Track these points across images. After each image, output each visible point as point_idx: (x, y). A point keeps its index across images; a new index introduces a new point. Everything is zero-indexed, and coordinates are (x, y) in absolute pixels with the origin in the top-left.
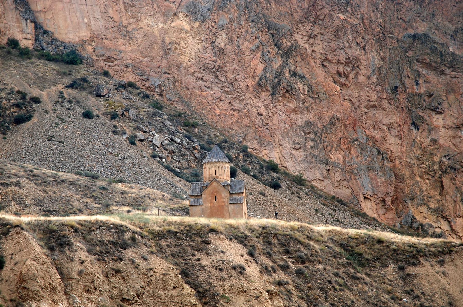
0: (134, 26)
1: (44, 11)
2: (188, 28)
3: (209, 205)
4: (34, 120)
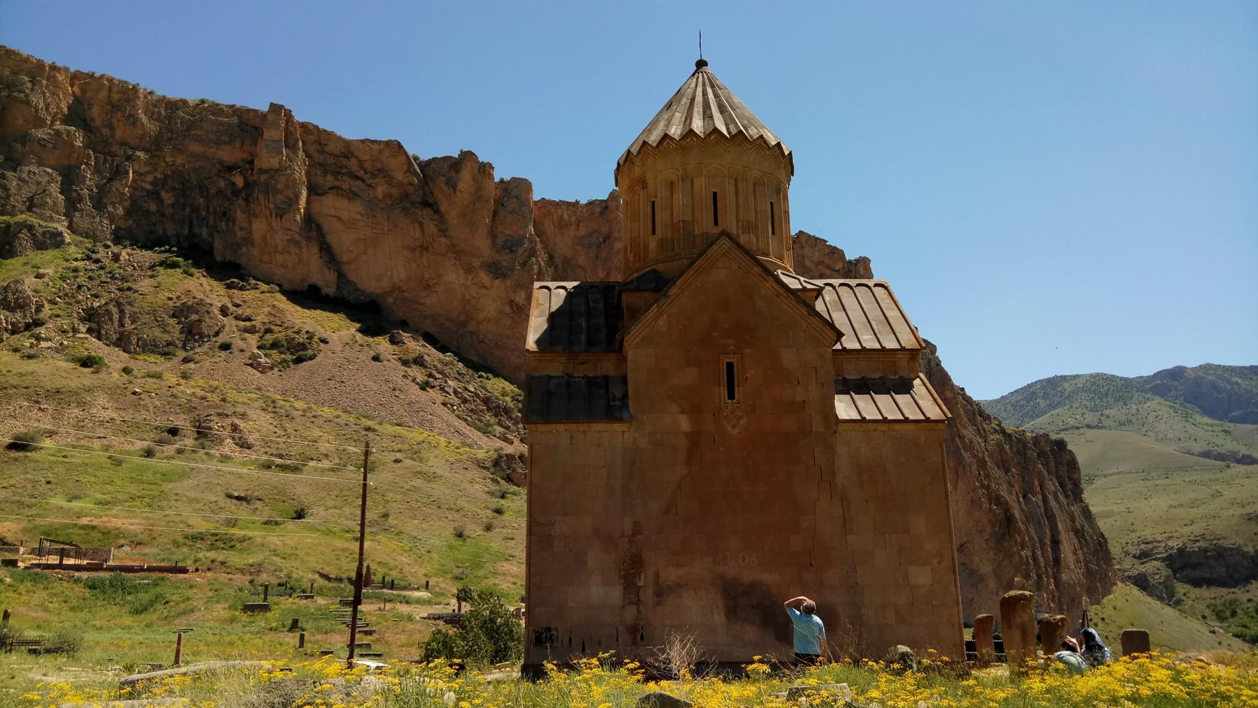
0: (436, 281)
1: (349, 263)
2: (487, 285)
3: (684, 423)
4: (318, 359)
